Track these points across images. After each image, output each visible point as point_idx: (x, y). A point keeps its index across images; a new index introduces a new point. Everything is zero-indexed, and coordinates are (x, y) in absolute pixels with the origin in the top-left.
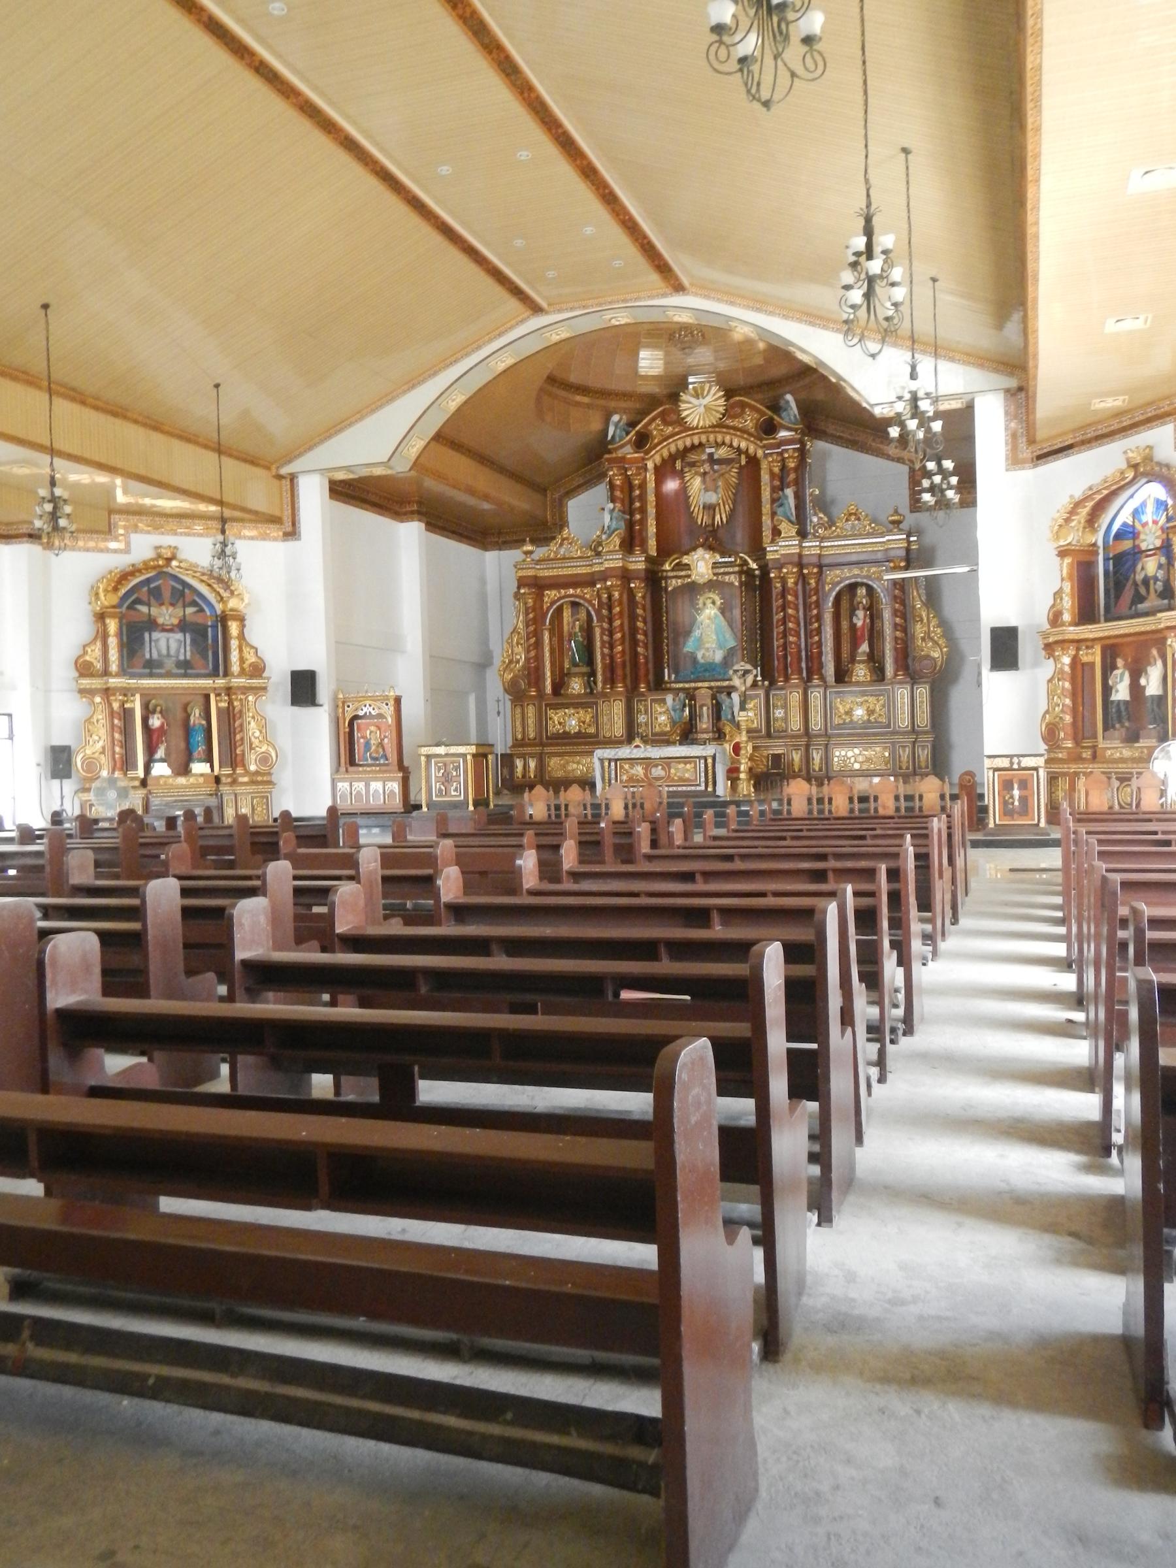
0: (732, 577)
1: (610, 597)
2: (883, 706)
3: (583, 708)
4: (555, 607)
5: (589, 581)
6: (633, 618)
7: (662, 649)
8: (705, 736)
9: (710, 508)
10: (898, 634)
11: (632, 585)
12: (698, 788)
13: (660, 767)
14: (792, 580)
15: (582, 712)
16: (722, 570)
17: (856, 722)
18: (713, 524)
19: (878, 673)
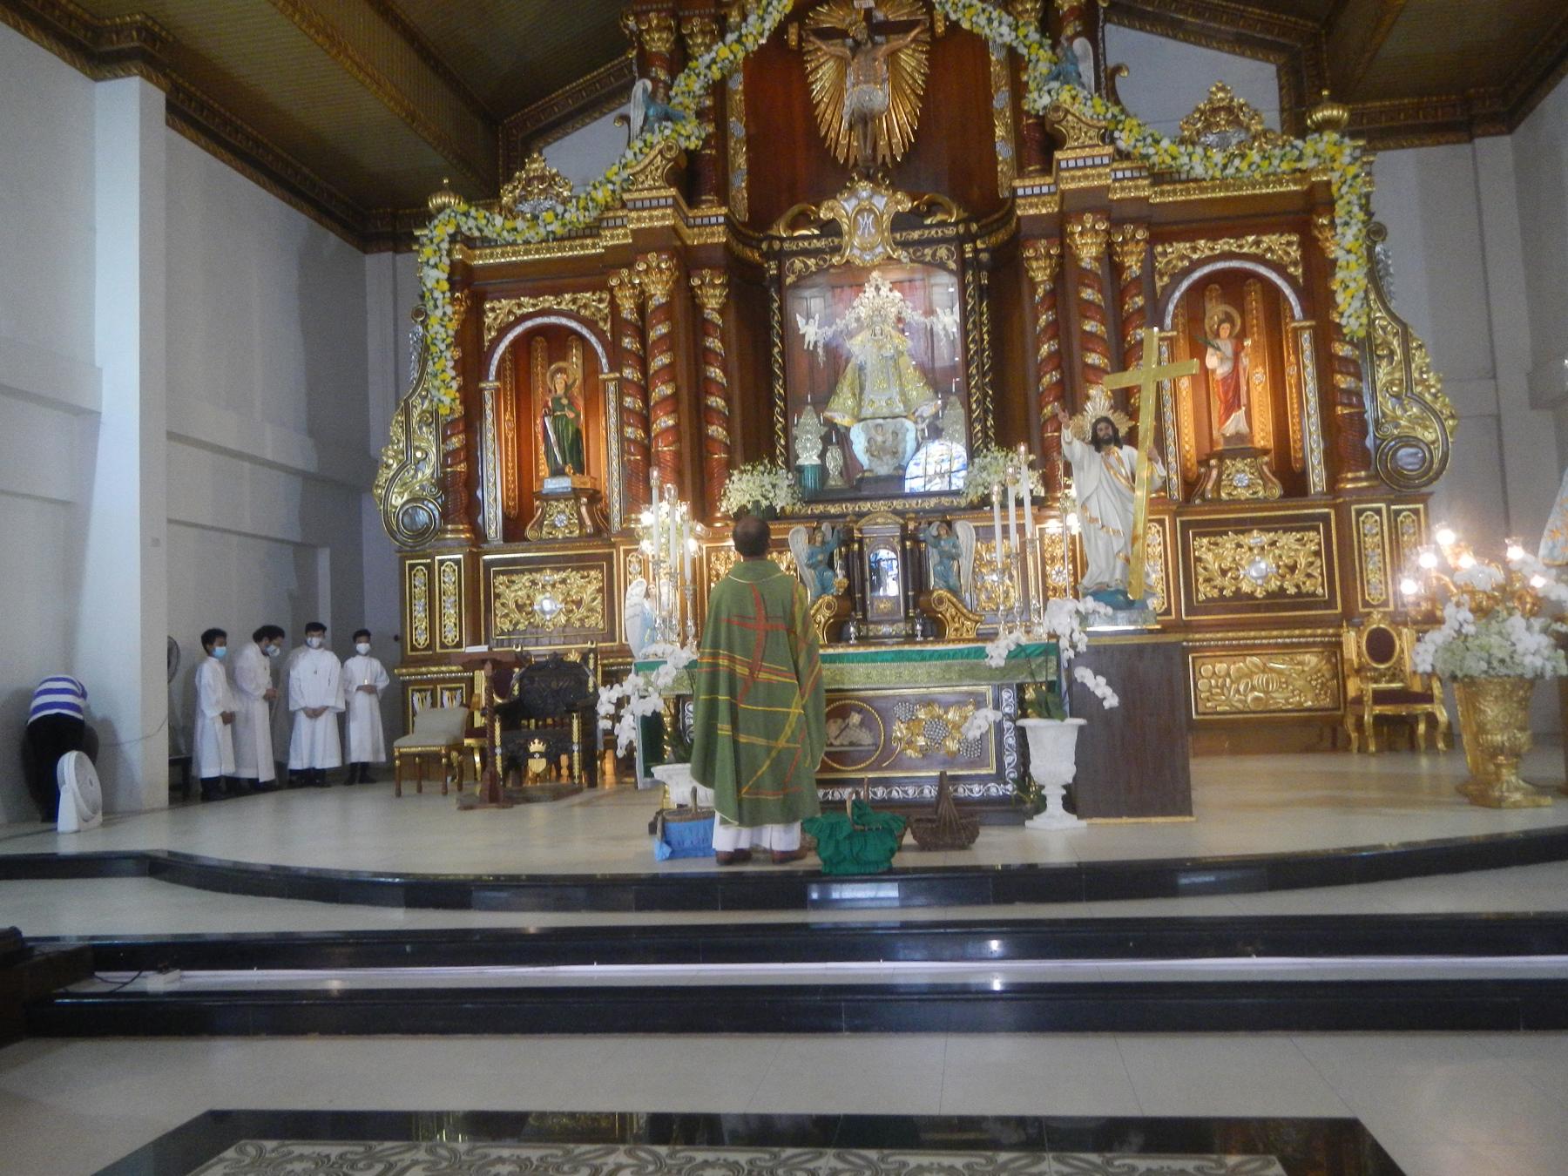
0: (942, 252)
1: (641, 309)
2: (1317, 554)
3: (578, 569)
4: (510, 337)
5: (592, 274)
6: (701, 356)
7: (772, 425)
8: (885, 629)
9: (864, 120)
10: (1343, 382)
11: (696, 282)
12: (995, 790)
13: (856, 718)
14: (1094, 251)
15: (575, 578)
16: (916, 235)
17: (1251, 596)
18: (874, 158)
19: (1293, 481)
